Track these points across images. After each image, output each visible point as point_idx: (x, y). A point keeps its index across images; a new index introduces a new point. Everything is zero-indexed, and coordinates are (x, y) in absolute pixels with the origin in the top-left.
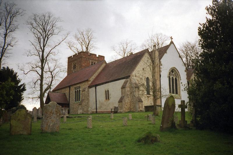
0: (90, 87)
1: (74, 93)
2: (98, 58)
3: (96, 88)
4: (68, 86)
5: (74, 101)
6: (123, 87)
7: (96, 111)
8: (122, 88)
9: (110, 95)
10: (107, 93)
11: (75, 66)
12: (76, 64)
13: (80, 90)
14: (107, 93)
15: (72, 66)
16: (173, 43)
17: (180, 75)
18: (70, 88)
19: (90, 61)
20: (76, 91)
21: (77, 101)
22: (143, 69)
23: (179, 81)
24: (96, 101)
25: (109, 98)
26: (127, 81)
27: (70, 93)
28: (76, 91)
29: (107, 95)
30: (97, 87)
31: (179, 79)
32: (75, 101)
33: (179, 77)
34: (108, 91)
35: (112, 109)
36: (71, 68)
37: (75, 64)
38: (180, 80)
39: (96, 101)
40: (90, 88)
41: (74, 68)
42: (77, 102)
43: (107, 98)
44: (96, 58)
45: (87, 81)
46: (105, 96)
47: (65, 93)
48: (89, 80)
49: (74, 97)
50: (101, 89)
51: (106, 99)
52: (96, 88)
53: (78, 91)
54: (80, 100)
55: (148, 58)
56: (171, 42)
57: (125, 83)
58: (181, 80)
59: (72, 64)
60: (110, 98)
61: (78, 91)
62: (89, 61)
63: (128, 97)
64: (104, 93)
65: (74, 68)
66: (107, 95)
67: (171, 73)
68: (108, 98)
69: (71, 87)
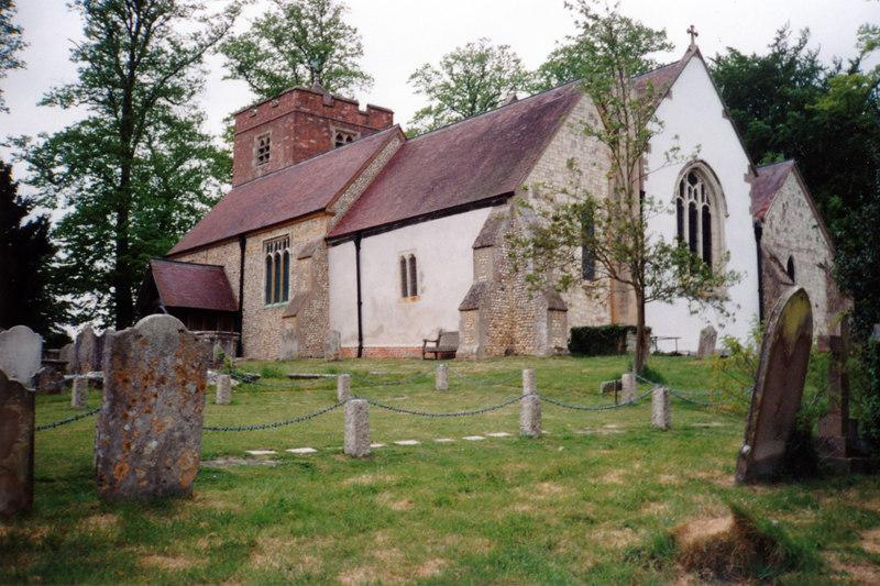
0: (333, 240)
2: (364, 118)
3: (358, 248)
5: (263, 302)
6: (482, 244)
7: (361, 348)
9: (422, 275)
10: (408, 267)
11: (268, 148)
12: (268, 142)
13: (286, 254)
14: (408, 267)
15: (255, 150)
16: (698, 53)
17: (723, 195)
19: (333, 129)
20: (272, 255)
21: (277, 300)
22: (570, 164)
23: (719, 222)
24: (360, 304)
25: (419, 293)
28: (269, 258)
30: (365, 242)
31: (722, 210)
32: (268, 301)
33: (721, 203)
34: (413, 260)
35: (425, 341)
36: (249, 159)
37: (265, 140)
38: (722, 215)
39: (360, 304)
40: (335, 245)
41: (261, 158)
42: (276, 304)
43: (409, 291)
44: (359, 117)
46: (398, 280)
47: (222, 267)
48: (328, 210)
49: (263, 283)
50: (382, 252)
51: (405, 294)
52: (358, 248)
53: (278, 256)
54: (291, 297)
55: (591, 116)
56: (689, 50)
57: (491, 225)
58: (727, 216)
59: (252, 141)
61: (278, 256)
62: (328, 131)
63: (503, 289)
65: (261, 158)
67: (688, 184)
68: (414, 292)
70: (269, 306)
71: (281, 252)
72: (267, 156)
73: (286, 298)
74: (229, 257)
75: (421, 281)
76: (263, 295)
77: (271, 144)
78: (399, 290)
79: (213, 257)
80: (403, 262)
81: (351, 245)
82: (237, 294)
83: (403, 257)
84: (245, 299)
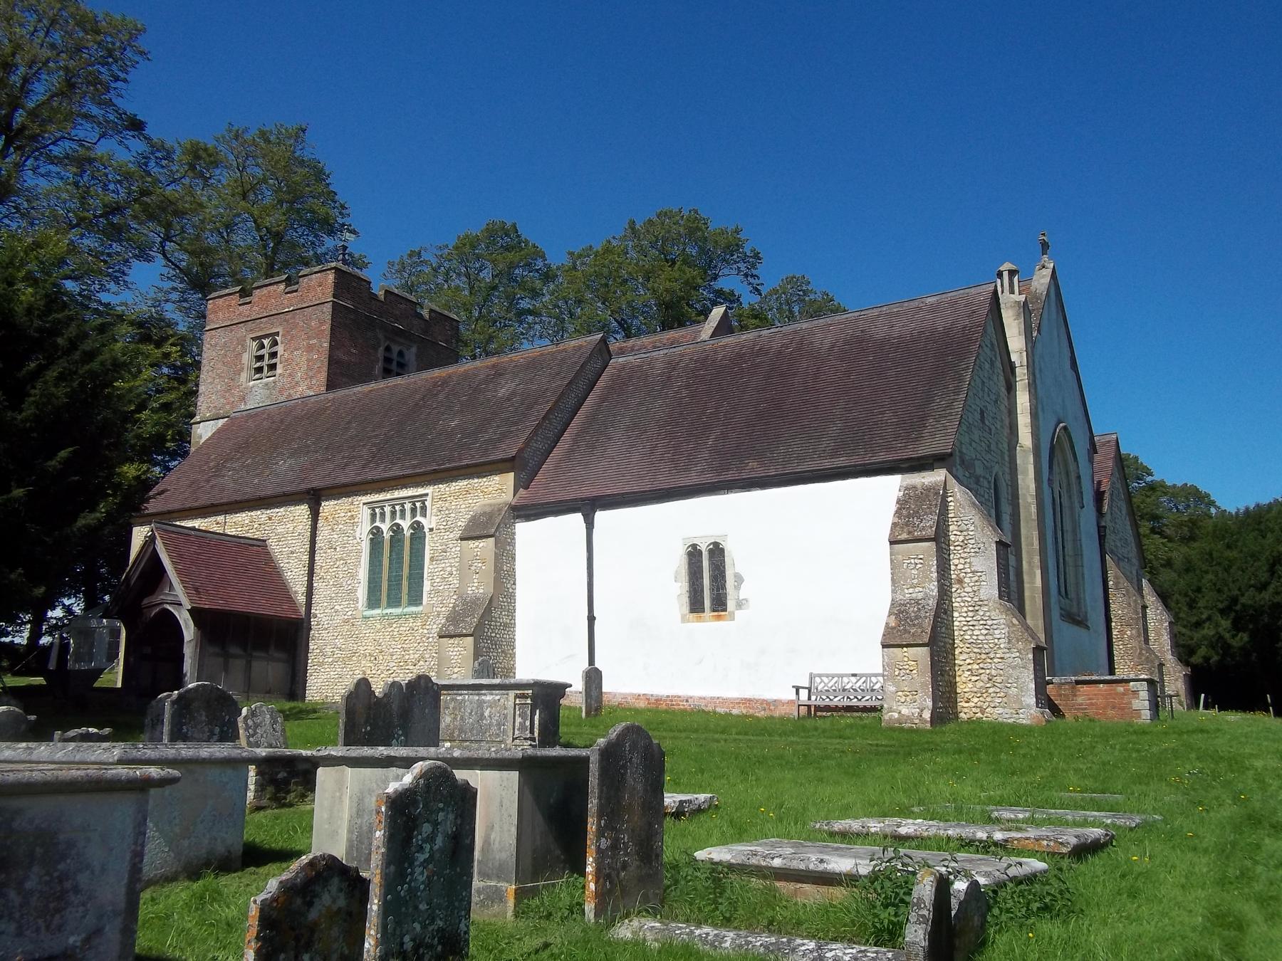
1: (365, 547)
4: (308, 492)
8: (892, 543)
9: (739, 579)
10: (706, 563)
11: (274, 355)
13: (417, 527)
14: (706, 563)
15: (246, 358)
20: (385, 527)
21: (394, 601)
22: (982, 413)
24: (591, 619)
25: (731, 604)
28: (376, 532)
29: (708, 582)
30: (601, 516)
32: (373, 602)
34: (717, 551)
39: (591, 619)
49: (363, 573)
51: (696, 606)
53: (397, 529)
59: (242, 342)
60: (740, 605)
61: (397, 529)
64: (678, 561)
66: (708, 582)
68: (720, 604)
69: (327, 507)
70: (377, 611)
71: (405, 524)
72: (272, 367)
73: (416, 599)
74: (283, 530)
75: (737, 588)
76: (362, 593)
77: (280, 349)
78: (685, 599)
79: (238, 524)
80: (694, 554)
81: (577, 519)
83: (694, 546)
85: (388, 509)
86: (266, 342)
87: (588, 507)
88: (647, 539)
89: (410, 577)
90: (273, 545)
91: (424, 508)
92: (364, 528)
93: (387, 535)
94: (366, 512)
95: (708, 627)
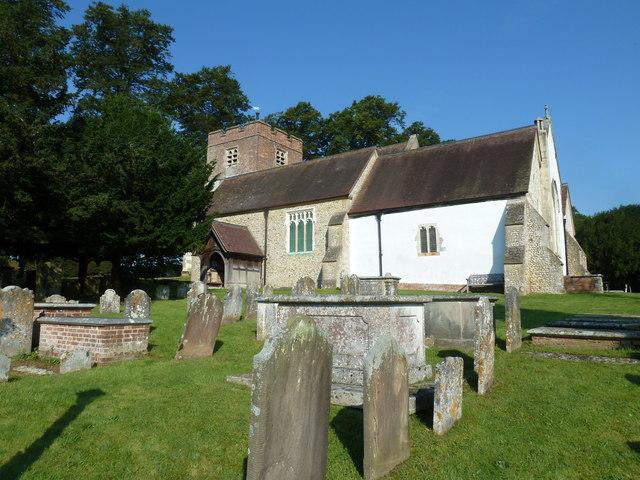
1: (289, 229)
10: (428, 234)
18: (266, 216)
24: (381, 255)
26: (520, 208)
27: (269, 227)
28: (292, 226)
29: (429, 241)
30: (384, 217)
32: (292, 249)
34: (433, 230)
37: (233, 151)
39: (381, 255)
40: (355, 217)
43: (429, 249)
45: (346, 196)
51: (424, 250)
53: (301, 223)
60: (441, 250)
61: (301, 223)
66: (429, 241)
68: (434, 249)
72: (235, 161)
73: (309, 248)
74: (253, 222)
80: (423, 231)
81: (372, 219)
82: (263, 248)
84: (268, 249)
85: (297, 215)
86: (233, 151)
87: (378, 213)
88: (403, 226)
89: (307, 241)
90: (250, 228)
91: (312, 215)
92: (288, 223)
93: (297, 224)
94: (288, 216)
95: (429, 258)
